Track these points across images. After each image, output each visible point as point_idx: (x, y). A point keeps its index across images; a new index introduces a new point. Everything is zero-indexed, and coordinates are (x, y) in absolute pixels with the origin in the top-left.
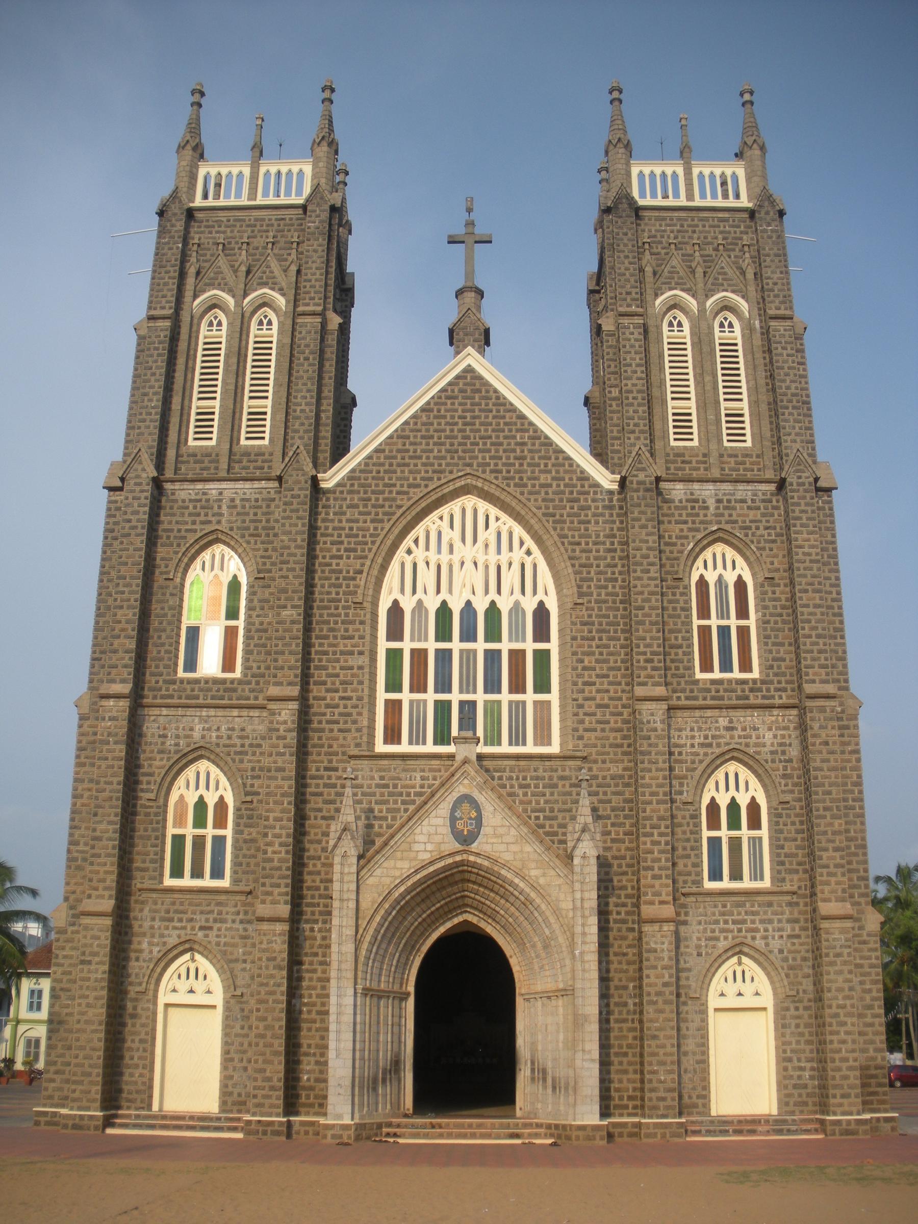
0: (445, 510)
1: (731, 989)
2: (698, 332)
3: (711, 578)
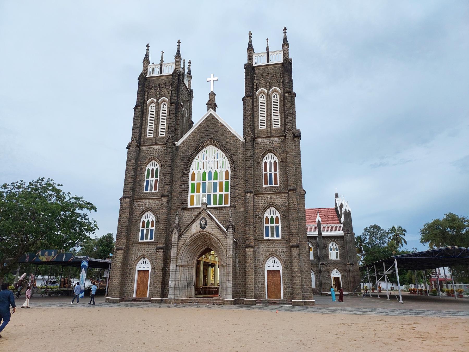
0: (205, 149)
1: (271, 265)
3: (268, 162)
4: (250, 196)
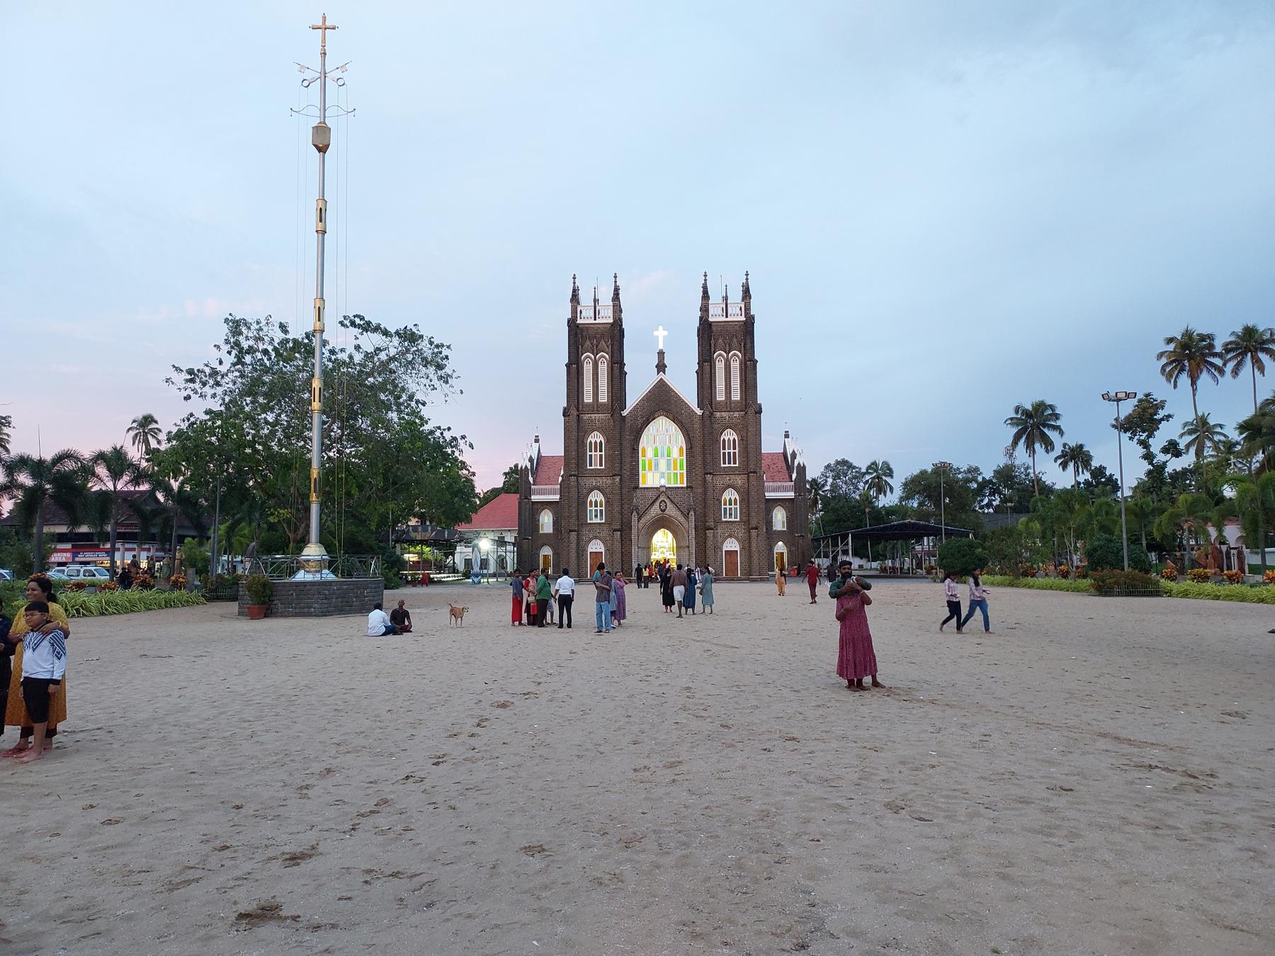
2: (727, 365)
4: (709, 477)
